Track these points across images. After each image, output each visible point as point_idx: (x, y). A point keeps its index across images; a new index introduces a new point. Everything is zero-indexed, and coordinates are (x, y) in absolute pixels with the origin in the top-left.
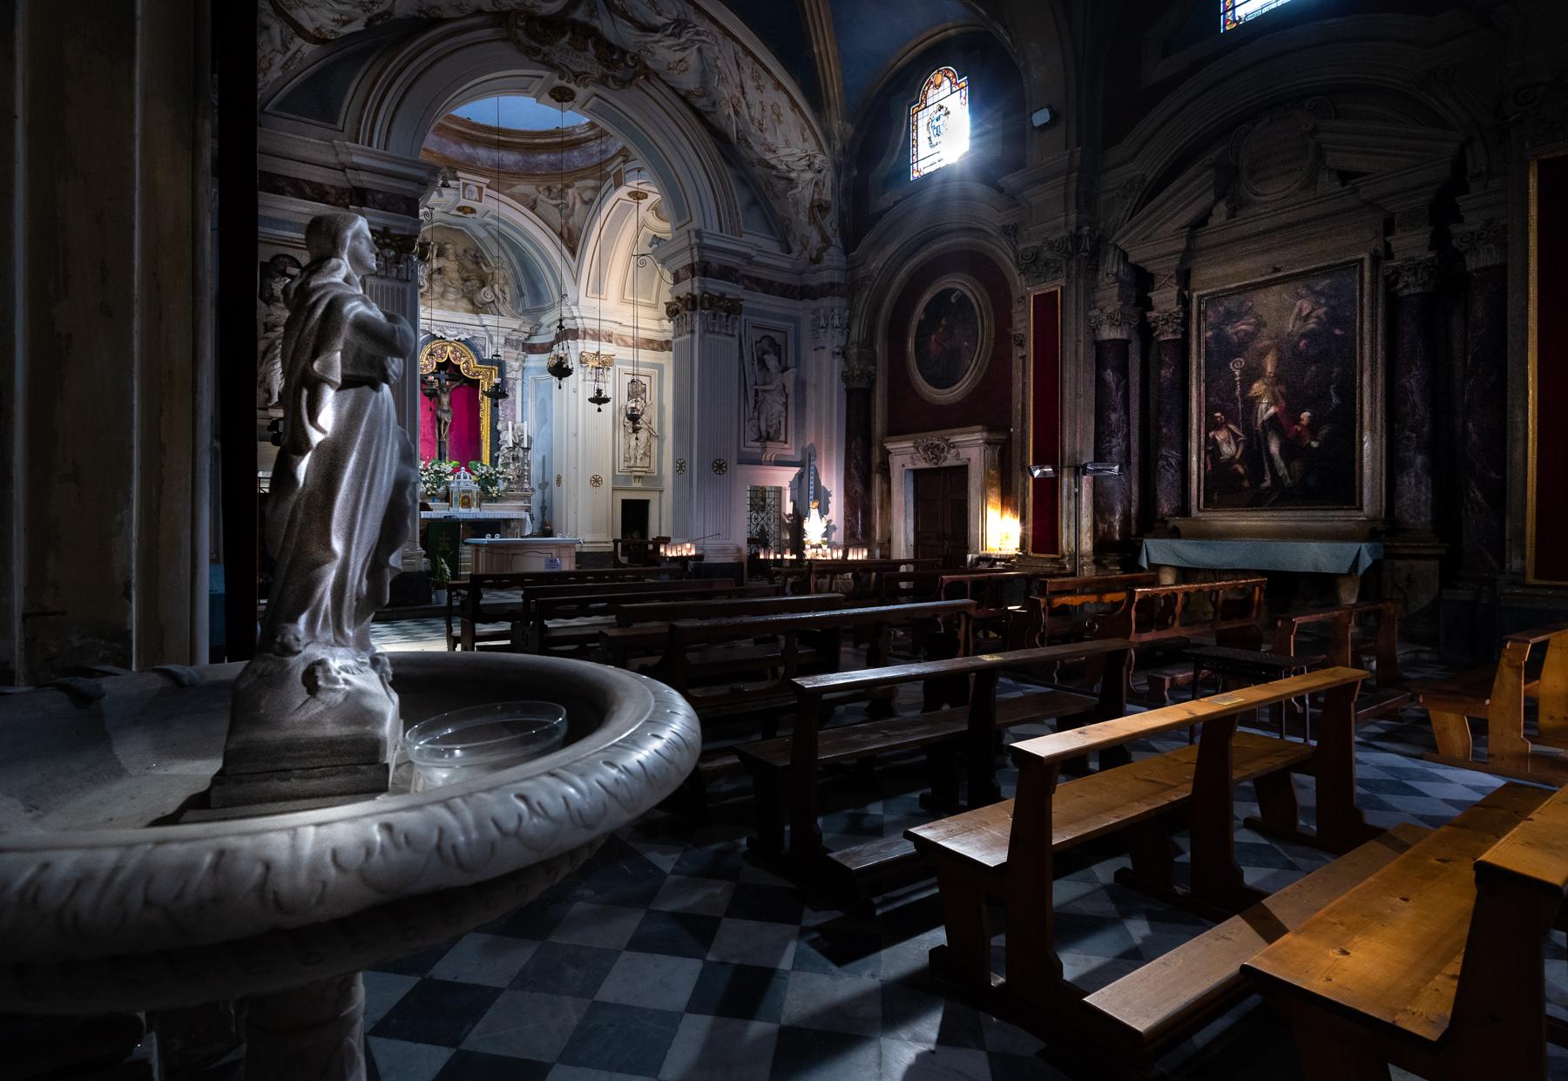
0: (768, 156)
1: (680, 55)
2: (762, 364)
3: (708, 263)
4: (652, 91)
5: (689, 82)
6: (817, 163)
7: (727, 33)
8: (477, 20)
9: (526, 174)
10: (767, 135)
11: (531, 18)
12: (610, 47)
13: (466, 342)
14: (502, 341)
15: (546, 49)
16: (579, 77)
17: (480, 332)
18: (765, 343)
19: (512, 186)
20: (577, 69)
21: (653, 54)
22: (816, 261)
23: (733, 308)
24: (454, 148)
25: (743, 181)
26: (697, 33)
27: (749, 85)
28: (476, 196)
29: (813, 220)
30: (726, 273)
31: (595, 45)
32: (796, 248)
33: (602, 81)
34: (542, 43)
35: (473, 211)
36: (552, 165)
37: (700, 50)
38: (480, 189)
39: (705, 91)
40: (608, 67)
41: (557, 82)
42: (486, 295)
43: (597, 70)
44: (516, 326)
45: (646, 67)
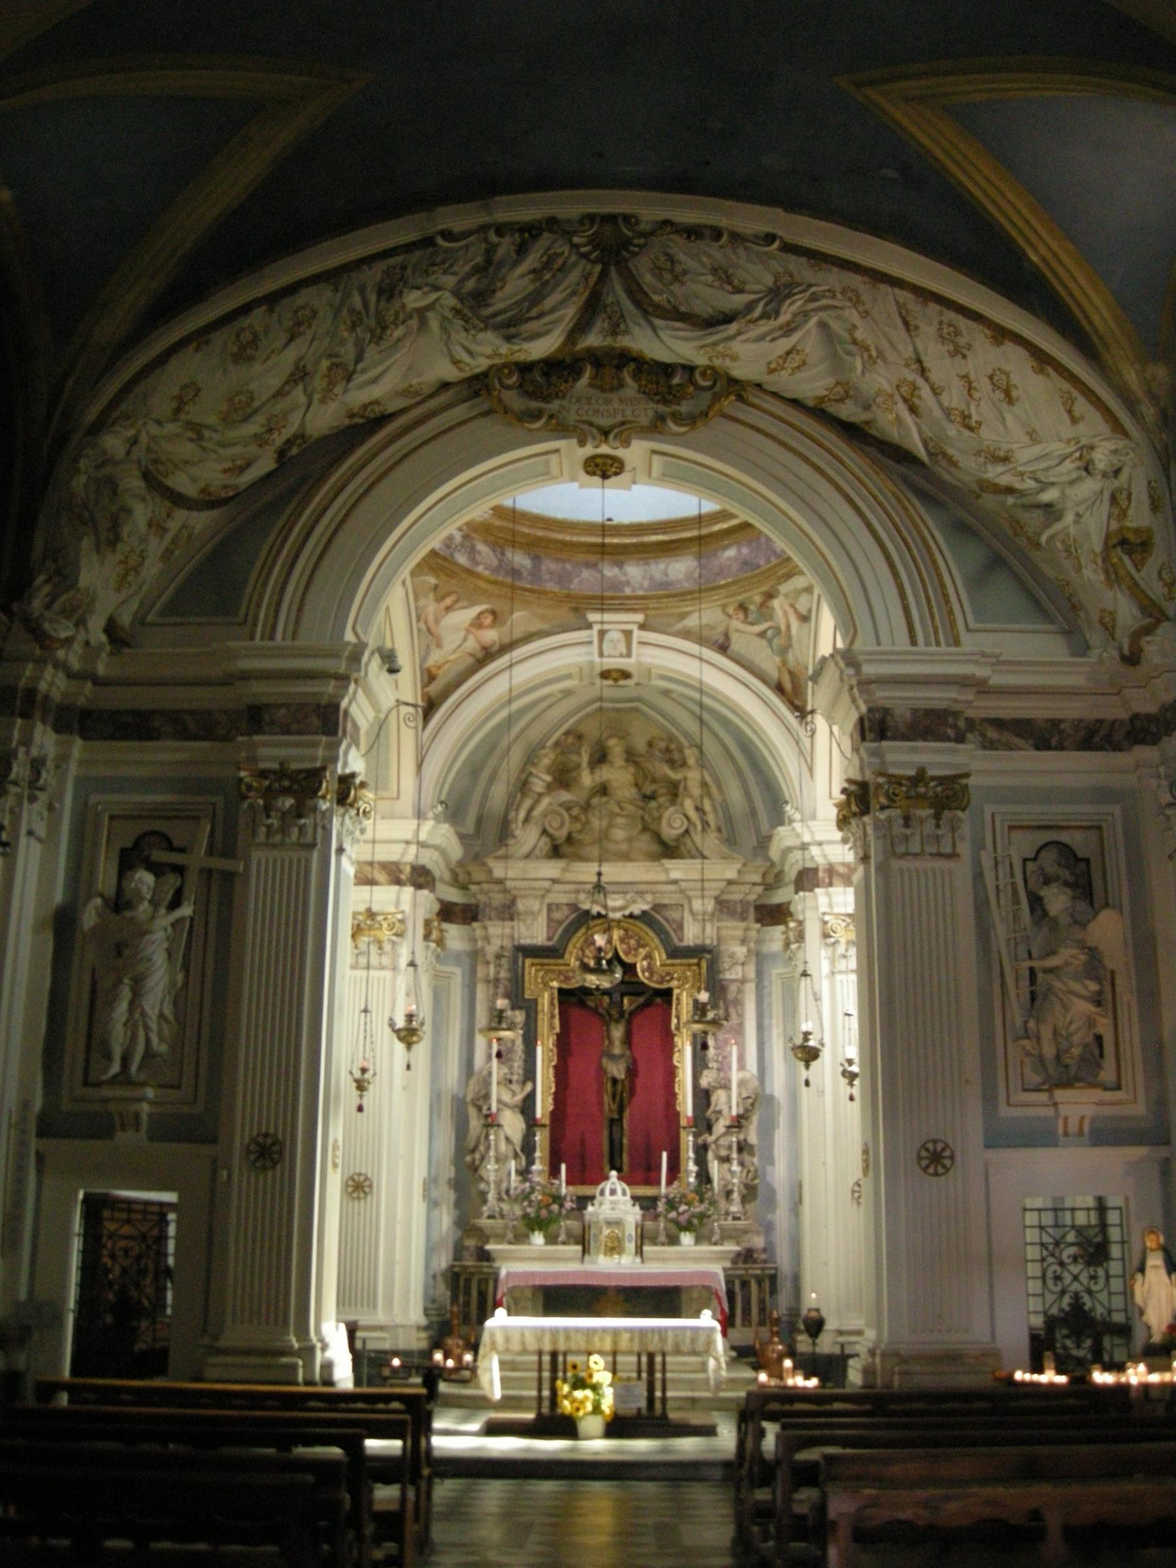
0: (997, 474)
1: (785, 344)
2: (1036, 902)
3: (886, 712)
4: (753, 416)
5: (812, 384)
6: (1101, 458)
7: (878, 277)
8: (444, 398)
9: (699, 592)
10: (985, 433)
11: (525, 368)
12: (667, 370)
13: (644, 917)
14: (710, 905)
15: (555, 406)
16: (621, 431)
18: (1049, 860)
19: (683, 616)
20: (605, 422)
21: (734, 358)
22: (1132, 659)
23: (949, 795)
24: (586, 574)
25: (962, 530)
26: (814, 298)
27: (934, 353)
28: (622, 648)
29: (1113, 576)
30: (930, 725)
31: (636, 376)
32: (1095, 637)
33: (656, 428)
34: (547, 399)
35: (626, 675)
36: (745, 563)
37: (823, 325)
38: (628, 634)
39: (847, 392)
40: (665, 402)
41: (589, 450)
43: (645, 411)
44: (731, 874)
45: (732, 381)
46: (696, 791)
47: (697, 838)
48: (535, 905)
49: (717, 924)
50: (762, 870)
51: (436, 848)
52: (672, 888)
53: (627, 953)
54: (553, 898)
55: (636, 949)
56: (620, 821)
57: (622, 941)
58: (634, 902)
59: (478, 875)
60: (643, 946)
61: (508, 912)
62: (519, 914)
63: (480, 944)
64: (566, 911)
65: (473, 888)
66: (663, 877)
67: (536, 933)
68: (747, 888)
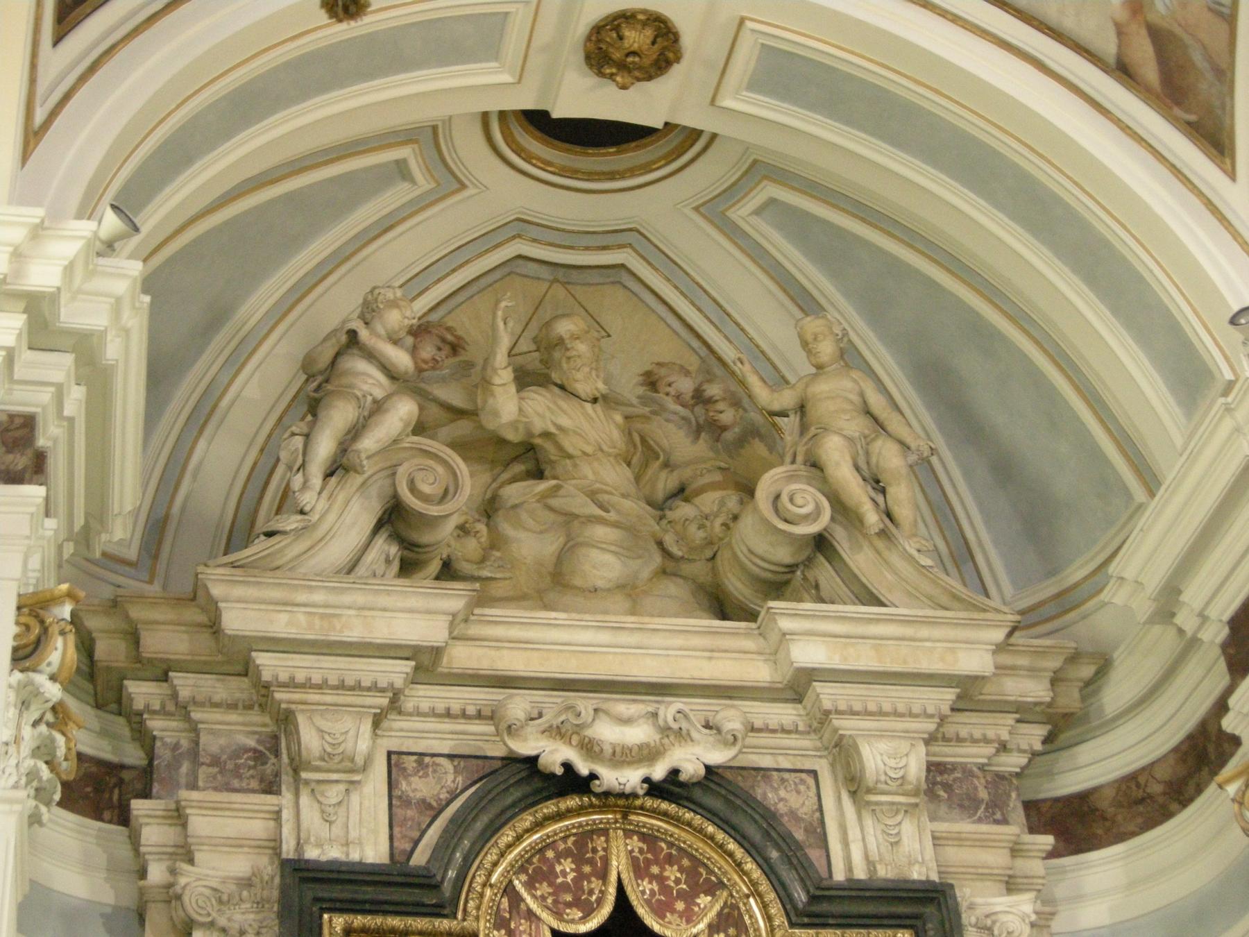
17: (771, 741)
42: (790, 501)
46: (856, 426)
47: (861, 560)
48: (360, 739)
49: (930, 826)
50: (1054, 663)
51: (85, 348)
52: (784, 714)
53: (660, 910)
54: (406, 734)
55: (689, 897)
56: (600, 532)
57: (640, 870)
58: (682, 736)
59: (167, 639)
60: (711, 889)
61: (271, 763)
62: (297, 766)
63: (157, 873)
64: (450, 776)
65: (141, 692)
66: (760, 673)
67: (355, 829)
68: (1002, 726)
